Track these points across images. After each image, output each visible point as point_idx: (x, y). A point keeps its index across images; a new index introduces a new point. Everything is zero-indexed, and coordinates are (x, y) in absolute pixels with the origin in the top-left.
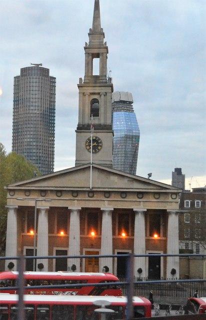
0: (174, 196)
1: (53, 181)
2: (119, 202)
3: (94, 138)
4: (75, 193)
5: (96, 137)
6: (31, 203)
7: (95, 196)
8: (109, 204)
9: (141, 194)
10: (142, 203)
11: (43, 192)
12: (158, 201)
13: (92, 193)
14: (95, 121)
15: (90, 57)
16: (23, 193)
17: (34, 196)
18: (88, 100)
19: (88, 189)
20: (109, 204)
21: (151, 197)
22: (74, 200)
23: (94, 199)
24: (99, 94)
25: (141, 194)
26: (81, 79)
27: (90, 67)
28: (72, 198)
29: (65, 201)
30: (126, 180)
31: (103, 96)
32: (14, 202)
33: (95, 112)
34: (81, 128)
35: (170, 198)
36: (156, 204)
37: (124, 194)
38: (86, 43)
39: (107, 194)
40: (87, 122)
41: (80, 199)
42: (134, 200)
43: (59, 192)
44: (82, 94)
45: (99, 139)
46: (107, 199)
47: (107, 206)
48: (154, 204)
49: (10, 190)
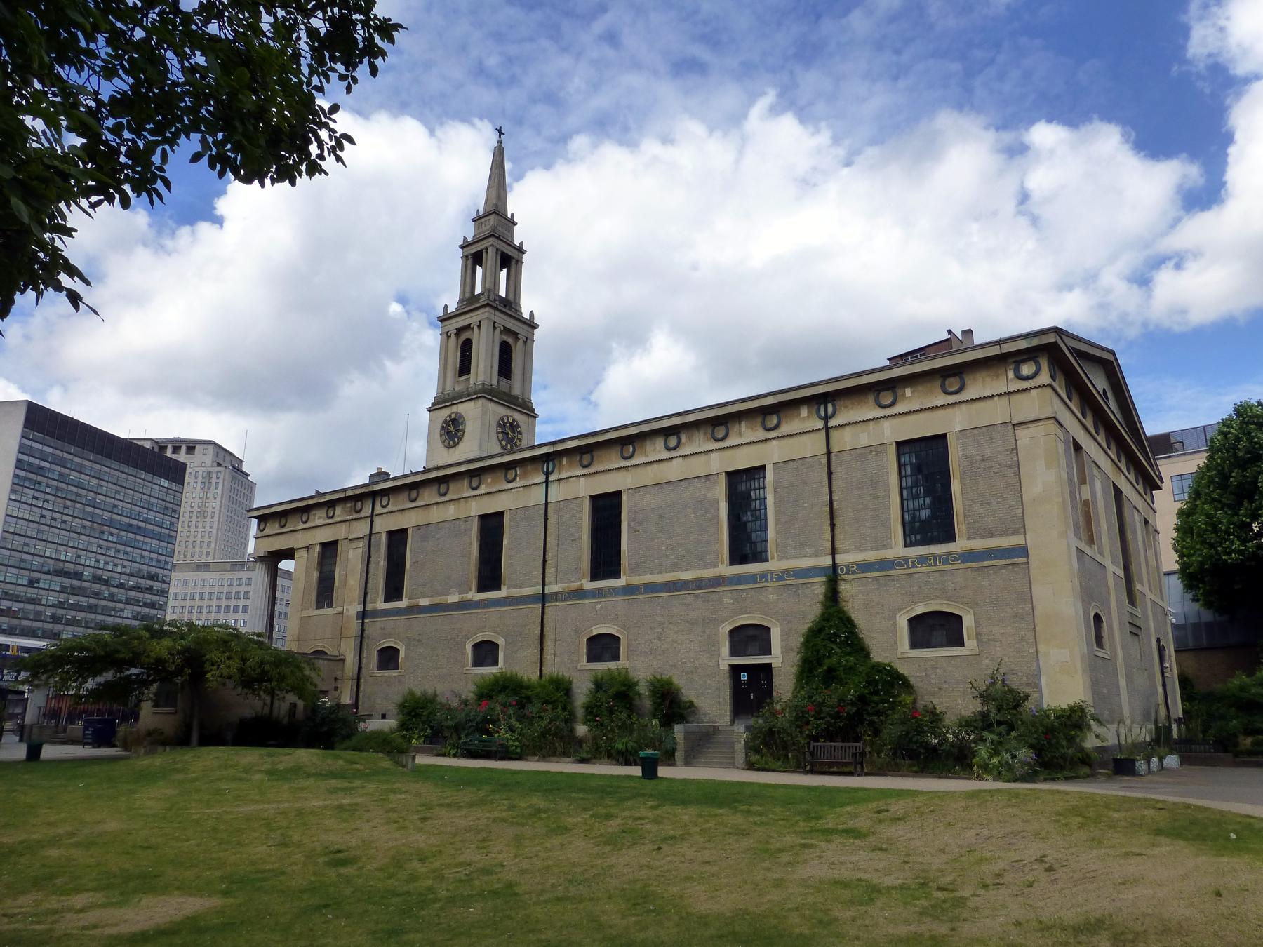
5: (456, 413)
15: (470, 262)
24: (468, 327)
26: (446, 307)
27: (468, 281)
31: (476, 329)
33: (464, 369)
38: (465, 239)
40: (449, 387)
45: (461, 416)
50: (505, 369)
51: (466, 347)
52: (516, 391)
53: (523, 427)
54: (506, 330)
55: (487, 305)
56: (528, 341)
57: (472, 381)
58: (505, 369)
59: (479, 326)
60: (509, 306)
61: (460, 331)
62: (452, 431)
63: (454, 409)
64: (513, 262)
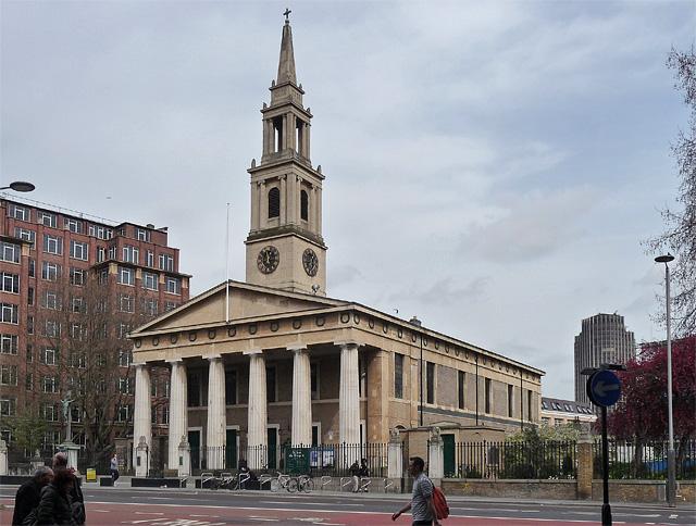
0: (345, 319)
1: (186, 317)
4: (212, 331)
5: (271, 247)
8: (255, 344)
9: (296, 321)
11: (174, 336)
12: (322, 328)
13: (231, 329)
14: (273, 224)
18: (265, 191)
19: (224, 324)
25: (296, 321)
30: (278, 302)
32: (141, 356)
33: (274, 211)
34: (252, 240)
35: (340, 322)
36: (319, 335)
37: (274, 324)
39: (252, 327)
43: (193, 334)
44: (256, 185)
46: (253, 336)
47: (251, 347)
48: (320, 337)
49: (137, 340)
50: (304, 215)
51: (274, 197)
52: (314, 230)
53: (319, 257)
54: (305, 182)
55: (293, 162)
56: (318, 189)
57: (283, 222)
58: (304, 215)
59: (285, 179)
60: (302, 161)
61: (268, 181)
62: (269, 261)
63: (269, 243)
64: (304, 126)
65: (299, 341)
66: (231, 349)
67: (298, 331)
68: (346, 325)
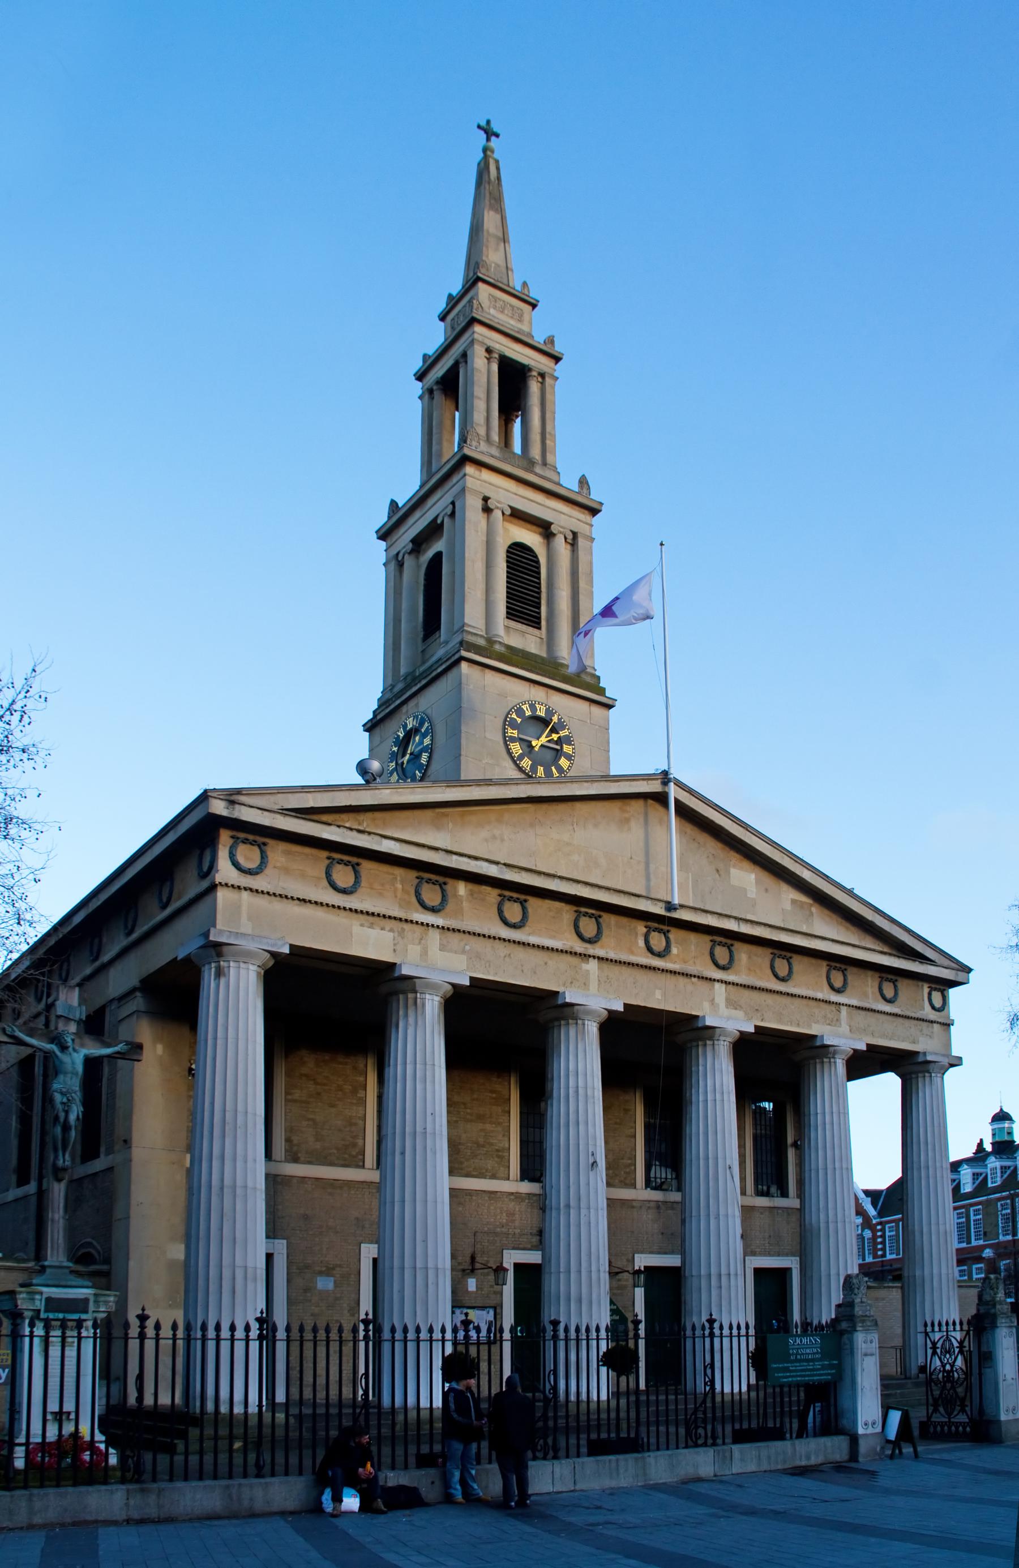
1: (484, 833)
2: (769, 999)
3: (541, 713)
6: (370, 943)
7: (674, 950)
10: (844, 1010)
16: (316, 862)
17: (385, 893)
19: (658, 910)
20: (731, 1003)
21: (870, 990)
22: (585, 957)
23: (670, 966)
28: (579, 947)
29: (540, 956)
30: (790, 895)
36: (889, 1025)
41: (612, 955)
42: (820, 995)
65: (844, 1028)
66: (660, 996)
67: (834, 998)
68: (933, 1015)
